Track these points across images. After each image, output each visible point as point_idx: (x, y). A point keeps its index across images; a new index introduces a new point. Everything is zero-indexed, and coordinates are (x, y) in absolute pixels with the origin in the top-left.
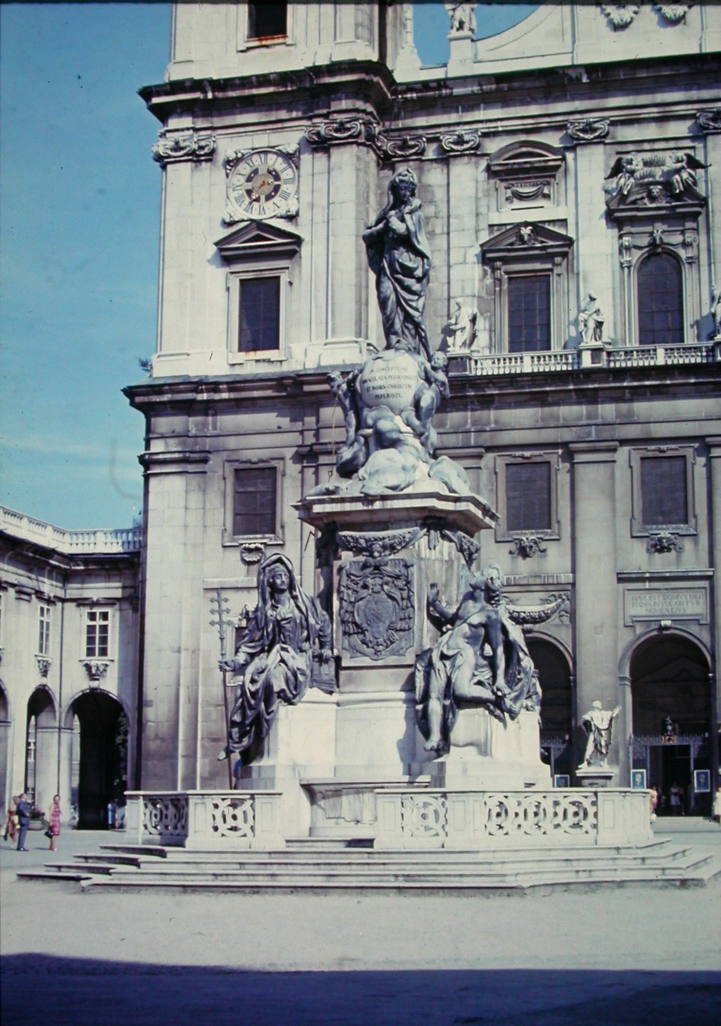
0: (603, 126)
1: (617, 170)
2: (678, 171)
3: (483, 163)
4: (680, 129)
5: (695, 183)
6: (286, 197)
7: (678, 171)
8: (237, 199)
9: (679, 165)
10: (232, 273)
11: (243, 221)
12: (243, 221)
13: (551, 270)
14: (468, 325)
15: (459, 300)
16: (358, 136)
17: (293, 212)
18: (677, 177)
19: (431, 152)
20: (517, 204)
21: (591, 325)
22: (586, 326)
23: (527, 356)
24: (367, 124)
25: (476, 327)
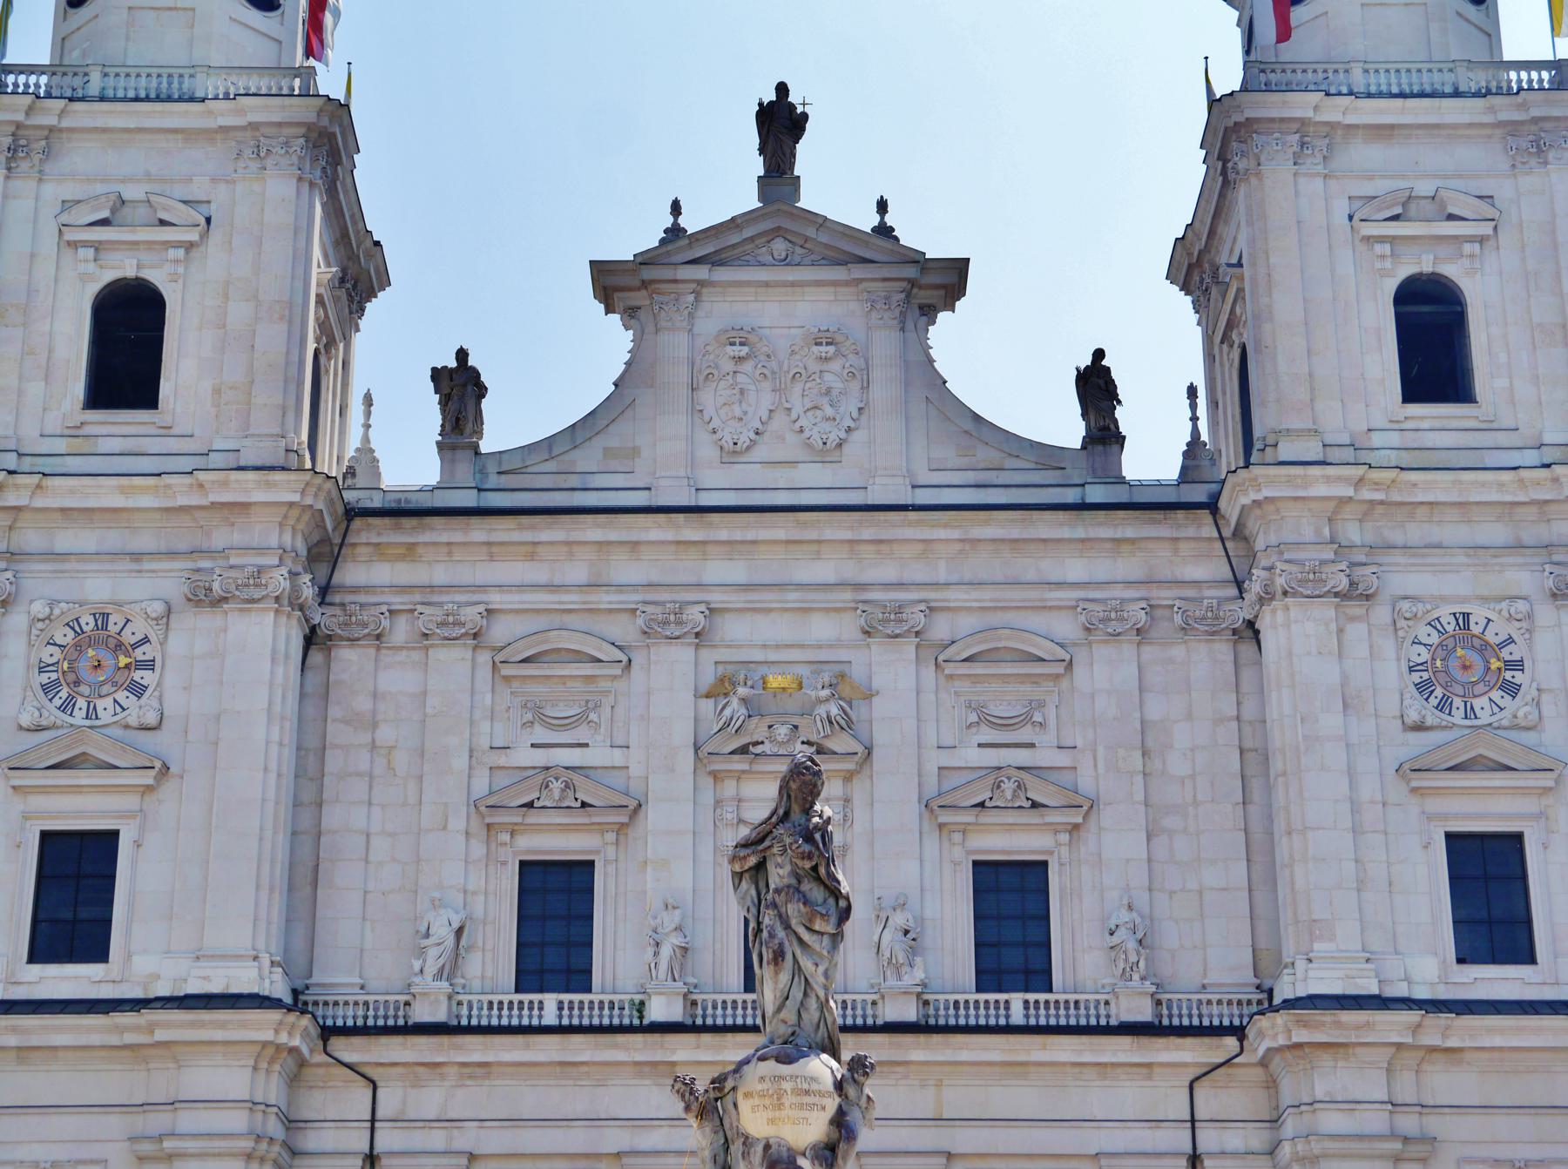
0: (695, 615)
1: (720, 689)
2: (820, 701)
3: (484, 658)
4: (822, 628)
5: (849, 722)
6: (138, 690)
7: (820, 701)
8: (46, 688)
9: (826, 693)
10: (26, 818)
11: (54, 727)
12: (54, 727)
13: (598, 852)
14: (450, 941)
15: (436, 894)
16: (277, 599)
17: (151, 718)
18: (821, 710)
19: (401, 631)
20: (541, 734)
21: (666, 951)
22: (656, 954)
23: (550, 1000)
24: (293, 575)
25: (463, 942)
